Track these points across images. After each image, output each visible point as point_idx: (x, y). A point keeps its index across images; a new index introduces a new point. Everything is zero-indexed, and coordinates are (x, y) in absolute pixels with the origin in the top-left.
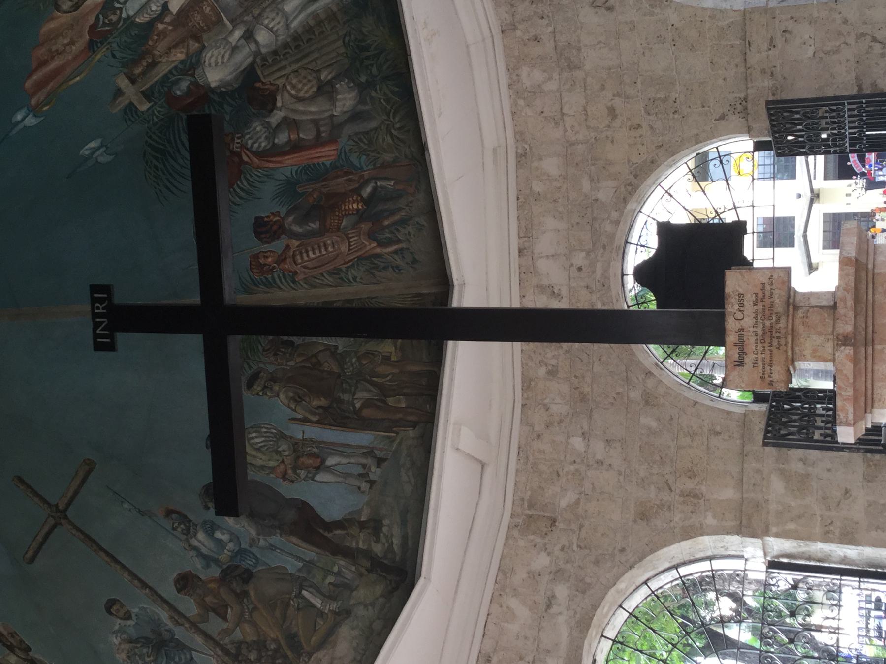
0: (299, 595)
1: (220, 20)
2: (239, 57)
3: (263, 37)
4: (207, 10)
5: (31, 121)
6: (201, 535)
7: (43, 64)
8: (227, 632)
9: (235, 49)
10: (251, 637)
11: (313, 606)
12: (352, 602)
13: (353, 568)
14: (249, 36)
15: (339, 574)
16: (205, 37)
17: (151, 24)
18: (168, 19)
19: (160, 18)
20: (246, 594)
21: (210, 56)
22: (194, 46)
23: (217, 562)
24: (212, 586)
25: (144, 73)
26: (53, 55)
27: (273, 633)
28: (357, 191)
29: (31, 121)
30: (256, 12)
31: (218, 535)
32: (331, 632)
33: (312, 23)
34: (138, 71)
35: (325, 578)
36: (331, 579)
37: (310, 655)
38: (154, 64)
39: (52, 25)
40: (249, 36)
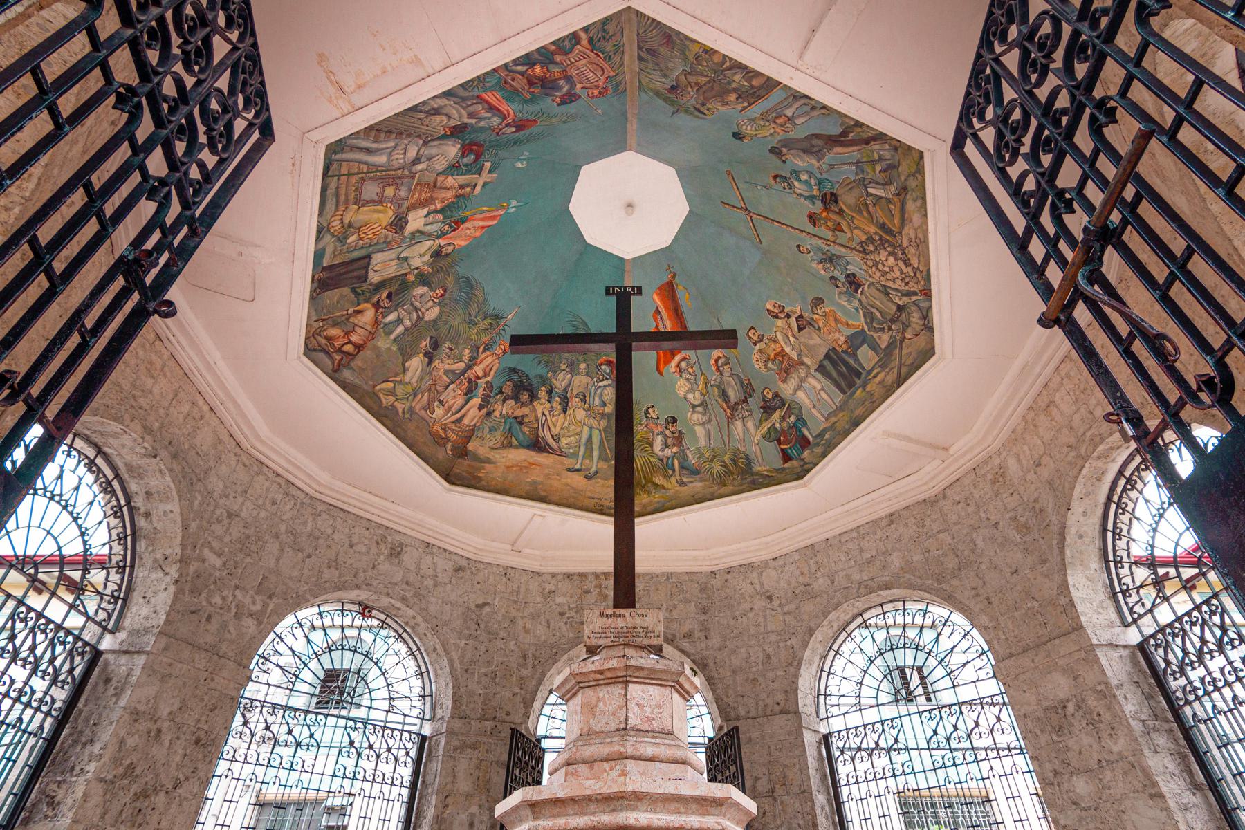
0: (869, 194)
1: (418, 184)
2: (434, 151)
3: (412, 153)
4: (416, 196)
5: (514, 203)
6: (796, 184)
7: (483, 227)
8: (851, 239)
9: (429, 159)
10: (864, 238)
11: (881, 197)
12: (903, 178)
13: (887, 146)
14: (417, 160)
15: (880, 159)
16: (432, 180)
17: (441, 211)
18: (433, 207)
19: (436, 211)
20: (841, 210)
21: (441, 164)
22: (440, 179)
23: (814, 197)
24: (824, 214)
25: (468, 186)
26: (476, 228)
27: (873, 229)
28: (522, 74)
29: (514, 203)
30: (399, 172)
31: (804, 177)
32: (903, 211)
33: (383, 135)
34: (469, 189)
35: (874, 170)
36: (878, 168)
37: (900, 233)
38: (461, 187)
39: (463, 243)
40: (417, 160)
